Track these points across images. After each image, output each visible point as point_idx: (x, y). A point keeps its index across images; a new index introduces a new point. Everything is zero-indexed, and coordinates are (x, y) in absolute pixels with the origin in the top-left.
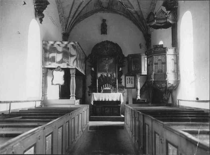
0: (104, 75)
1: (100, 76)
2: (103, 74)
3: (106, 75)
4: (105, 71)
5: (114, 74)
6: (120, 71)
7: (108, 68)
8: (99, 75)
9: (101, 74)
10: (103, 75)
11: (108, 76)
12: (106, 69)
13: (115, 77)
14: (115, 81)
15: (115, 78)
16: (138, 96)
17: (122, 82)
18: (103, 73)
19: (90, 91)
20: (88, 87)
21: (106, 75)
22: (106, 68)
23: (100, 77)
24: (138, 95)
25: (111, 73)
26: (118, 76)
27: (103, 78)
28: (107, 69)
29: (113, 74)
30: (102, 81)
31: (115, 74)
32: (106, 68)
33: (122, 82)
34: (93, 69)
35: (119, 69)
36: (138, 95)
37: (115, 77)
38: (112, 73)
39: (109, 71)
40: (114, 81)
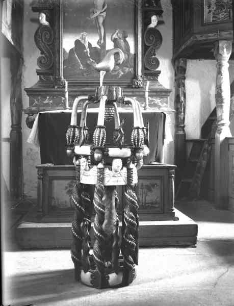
0: (90, 45)
1: (73, 46)
2: (84, 39)
3: (95, 44)
4: (93, 28)
5: (127, 39)
6: (152, 29)
7: (104, 14)
8: (68, 43)
9: (78, 37)
10: (87, 45)
11: (103, 46)
12: (97, 18)
13: (132, 51)
14: (132, 70)
15: (132, 57)
16: (223, 125)
17: (159, 72)
18: (85, 33)
19: (34, 109)
20: (26, 93)
21: (99, 42)
22: (95, 15)
23: (72, 50)
24: (222, 122)
25: (115, 36)
26: (145, 48)
27: (83, 57)
28: (101, 20)
29: (125, 37)
30: (81, 67)
31: (130, 41)
32: (95, 15)
33: (159, 72)
34: (43, 19)
35: (147, 22)
36: (222, 122)
37: (132, 51)
38: (121, 37)
39: (109, 25)
40: (127, 70)
